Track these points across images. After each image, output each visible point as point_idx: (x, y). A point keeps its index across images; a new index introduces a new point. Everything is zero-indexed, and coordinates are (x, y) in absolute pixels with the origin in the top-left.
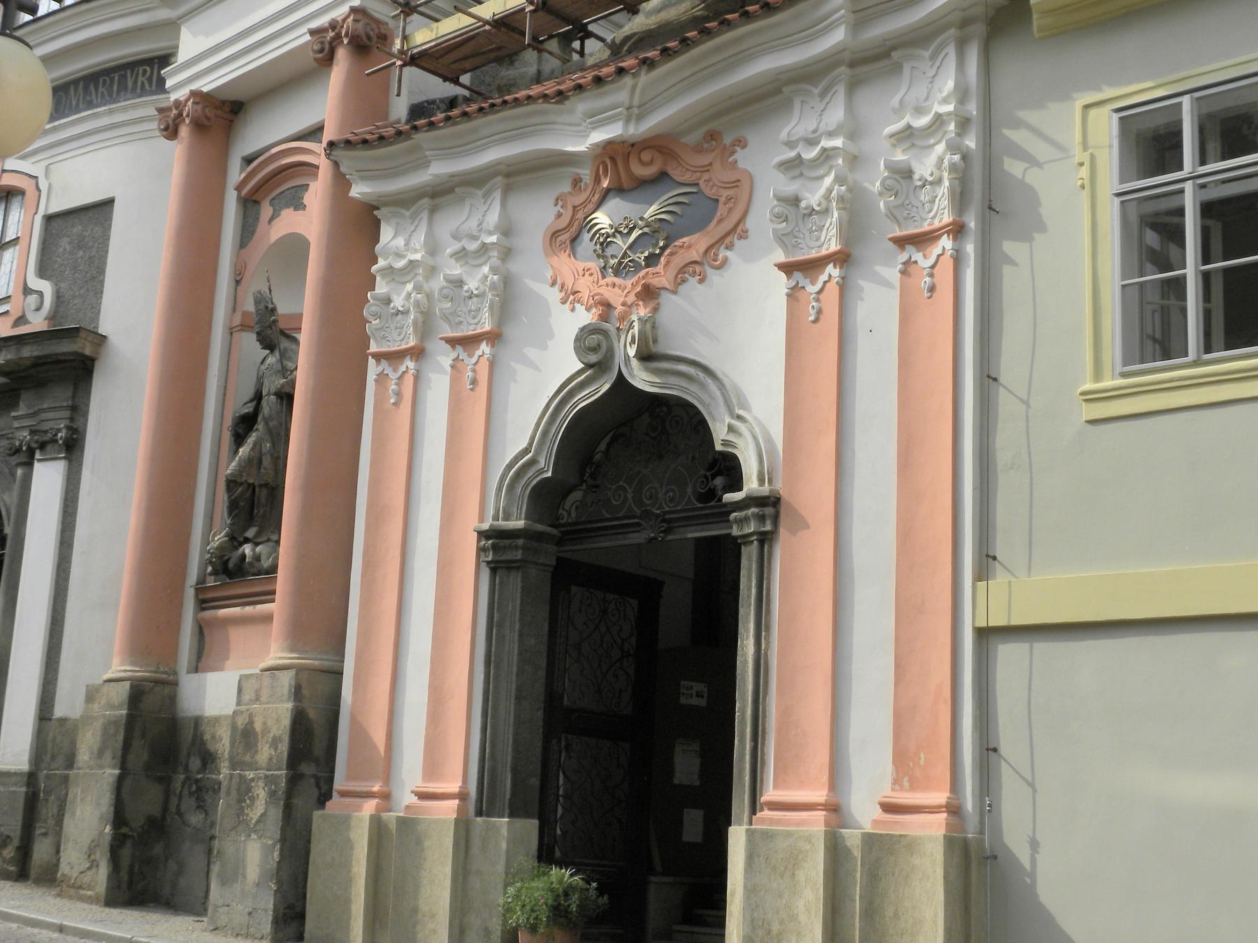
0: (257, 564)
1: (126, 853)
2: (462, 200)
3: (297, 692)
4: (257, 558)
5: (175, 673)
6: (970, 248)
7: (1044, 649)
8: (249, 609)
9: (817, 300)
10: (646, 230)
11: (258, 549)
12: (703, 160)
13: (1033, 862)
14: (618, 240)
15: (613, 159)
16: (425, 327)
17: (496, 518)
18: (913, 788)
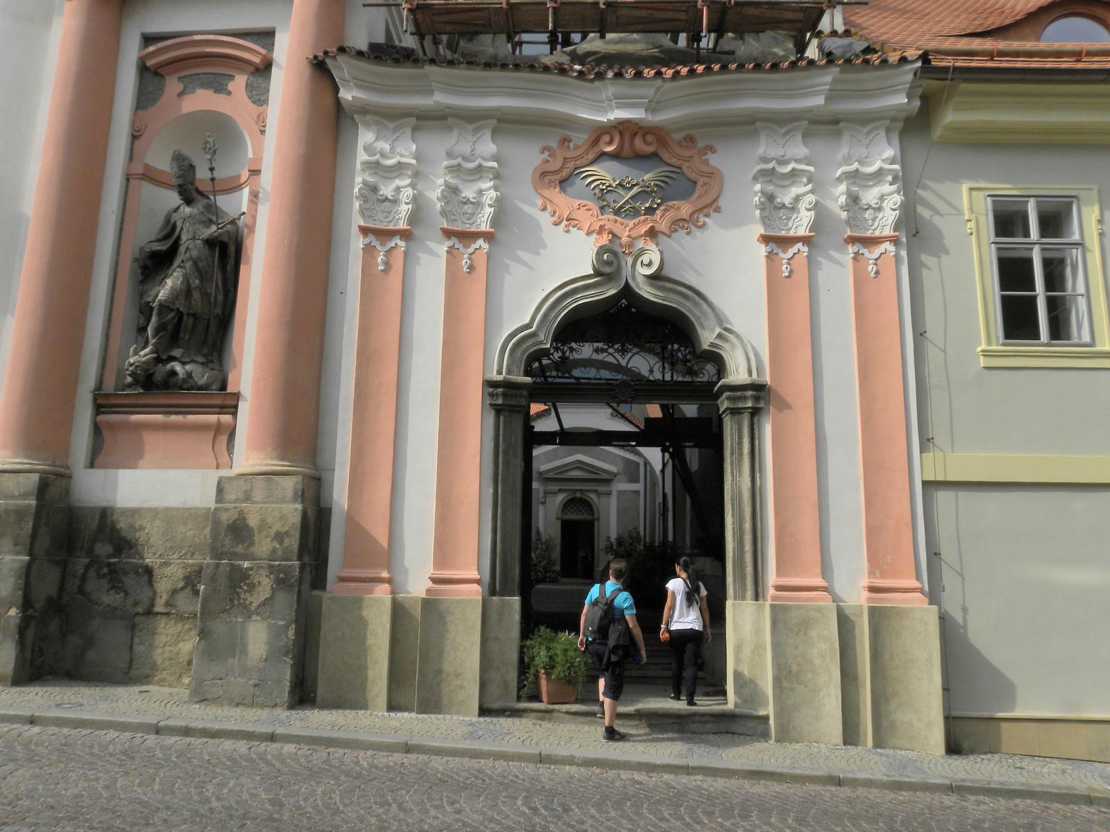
0: (190, 380)
1: (31, 632)
2: (450, 129)
3: (302, 496)
4: (189, 375)
5: (69, 468)
6: (904, 253)
7: (964, 496)
8: (174, 418)
9: (875, 264)
10: (646, 189)
11: (188, 367)
12: (688, 153)
13: (965, 620)
14: (620, 191)
15: (621, 133)
16: (414, 218)
17: (499, 372)
18: (883, 577)
